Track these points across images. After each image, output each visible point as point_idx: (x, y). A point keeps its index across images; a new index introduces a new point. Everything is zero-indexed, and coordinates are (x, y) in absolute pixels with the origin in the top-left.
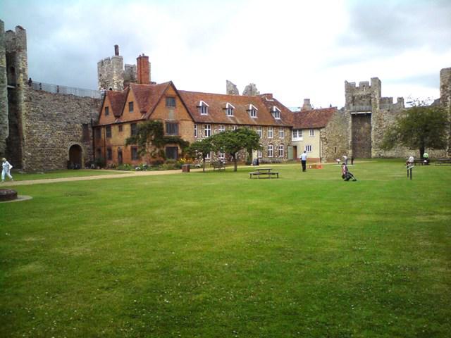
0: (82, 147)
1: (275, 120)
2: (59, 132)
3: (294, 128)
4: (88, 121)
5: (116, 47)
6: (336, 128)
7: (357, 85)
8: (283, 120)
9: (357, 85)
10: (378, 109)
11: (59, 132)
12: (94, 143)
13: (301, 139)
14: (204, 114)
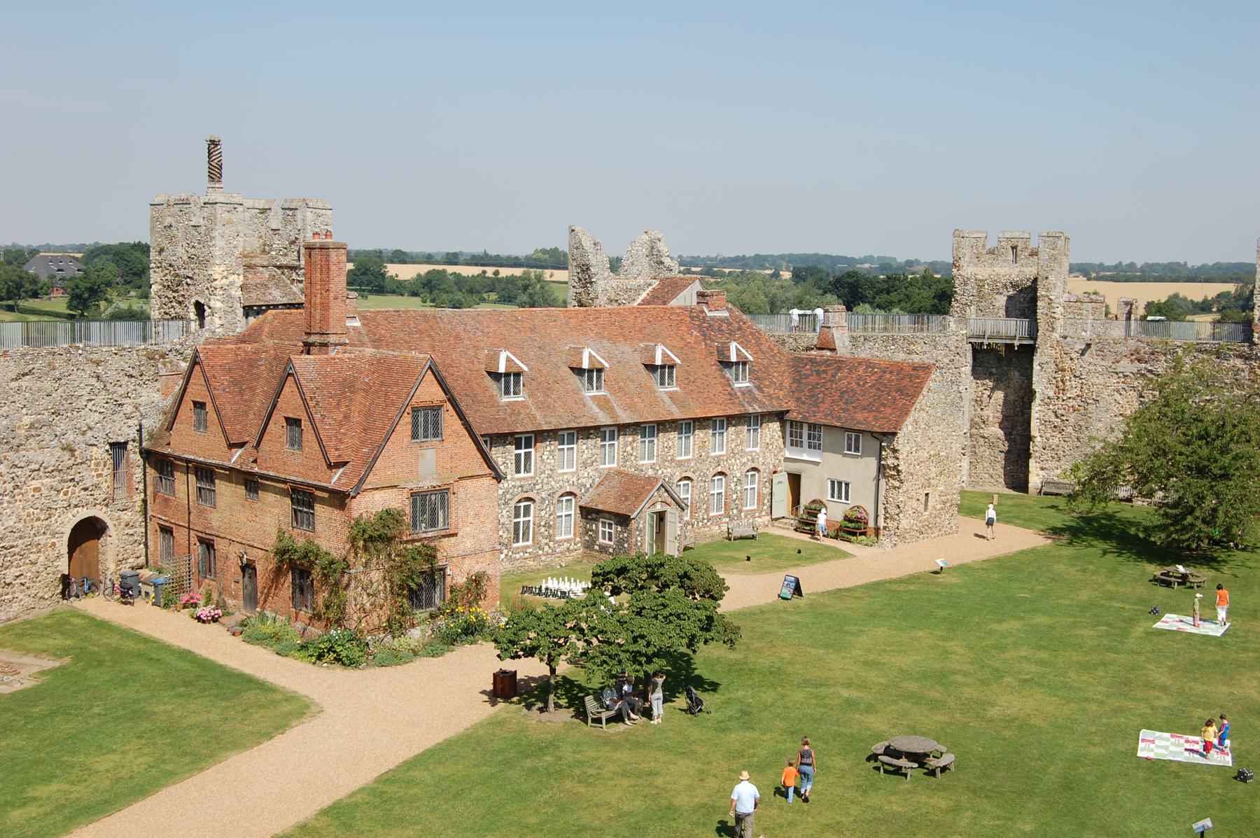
0: (110, 524)
1: (732, 395)
2: (35, 484)
3: (792, 416)
4: (127, 432)
6: (930, 433)
7: (992, 244)
8: (759, 388)
11: (35, 484)
12: (145, 501)
14: (511, 398)
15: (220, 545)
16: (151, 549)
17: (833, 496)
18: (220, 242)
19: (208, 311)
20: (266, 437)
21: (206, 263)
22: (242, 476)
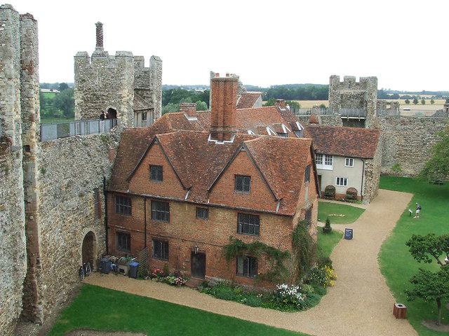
5: (99, 27)
7: (342, 80)
9: (342, 80)
10: (375, 115)
13: (329, 167)
15: (173, 244)
16: (110, 242)
17: (338, 184)
18: (127, 77)
19: (118, 114)
20: (218, 185)
21: (119, 87)
22: (193, 208)
